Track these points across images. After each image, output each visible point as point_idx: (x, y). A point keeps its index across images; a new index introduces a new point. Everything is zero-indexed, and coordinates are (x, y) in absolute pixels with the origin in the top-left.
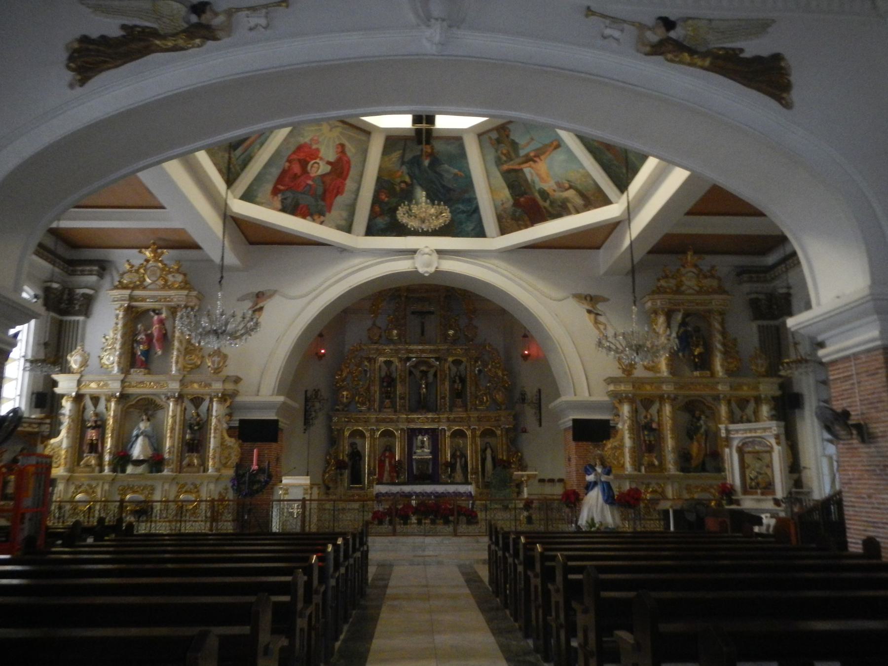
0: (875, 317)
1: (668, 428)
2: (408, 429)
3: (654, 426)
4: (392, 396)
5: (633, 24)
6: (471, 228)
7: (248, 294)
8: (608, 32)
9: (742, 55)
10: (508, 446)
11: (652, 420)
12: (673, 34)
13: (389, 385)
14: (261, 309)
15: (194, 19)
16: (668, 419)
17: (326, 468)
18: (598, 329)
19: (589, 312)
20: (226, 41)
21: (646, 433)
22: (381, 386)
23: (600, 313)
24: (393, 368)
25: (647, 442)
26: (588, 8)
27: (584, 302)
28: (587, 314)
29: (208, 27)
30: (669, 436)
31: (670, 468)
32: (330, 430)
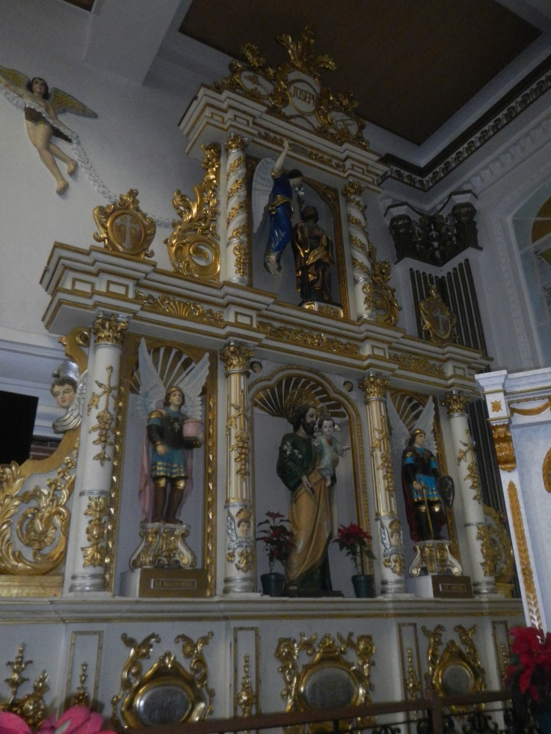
1: (234, 442)
3: (190, 430)
11: (181, 419)
16: (233, 412)
18: (54, 168)
21: (161, 449)
23: (62, 129)
25: (162, 482)
27: (23, 91)
28: (25, 124)
30: (234, 467)
31: (227, 581)
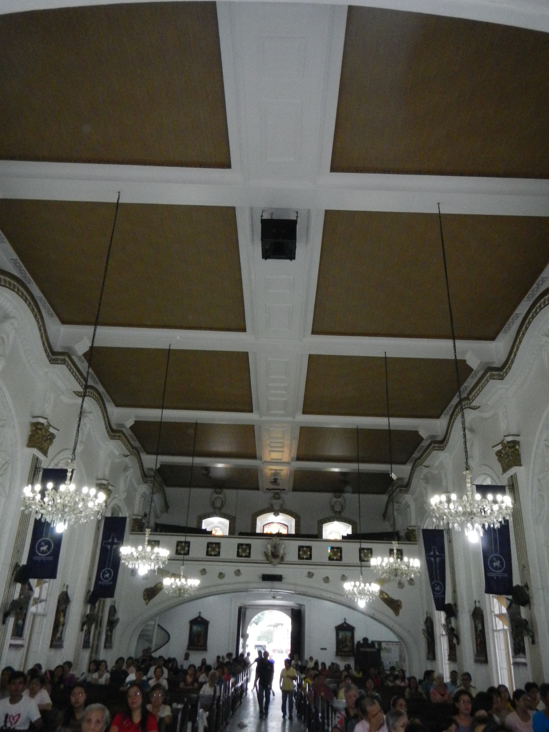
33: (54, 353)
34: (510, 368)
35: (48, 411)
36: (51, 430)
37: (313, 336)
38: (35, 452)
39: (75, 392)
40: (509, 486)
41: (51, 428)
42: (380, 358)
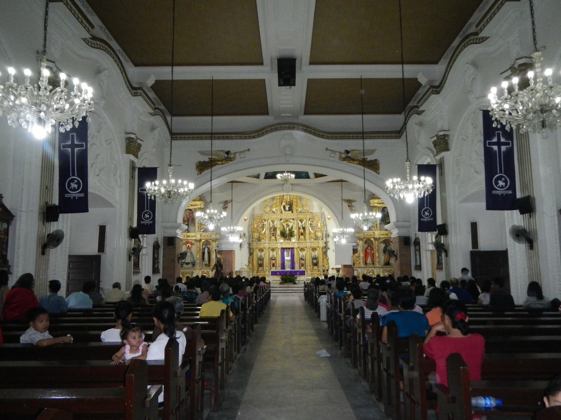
0: (397, 229)
2: (282, 248)
4: (275, 235)
5: (338, 152)
6: (304, 175)
7: (222, 202)
8: (332, 155)
9: (367, 160)
10: (323, 255)
12: (349, 155)
13: (274, 231)
14: (227, 207)
15: (226, 155)
17: (249, 264)
19: (349, 206)
20: (234, 162)
22: (270, 231)
24: (275, 224)
26: (327, 148)
29: (230, 158)
32: (250, 249)
33: (134, 88)
34: (443, 87)
35: (136, 130)
36: (139, 141)
37: (310, 66)
38: (132, 157)
39: (149, 113)
40: (439, 164)
41: (138, 140)
42: (359, 79)
